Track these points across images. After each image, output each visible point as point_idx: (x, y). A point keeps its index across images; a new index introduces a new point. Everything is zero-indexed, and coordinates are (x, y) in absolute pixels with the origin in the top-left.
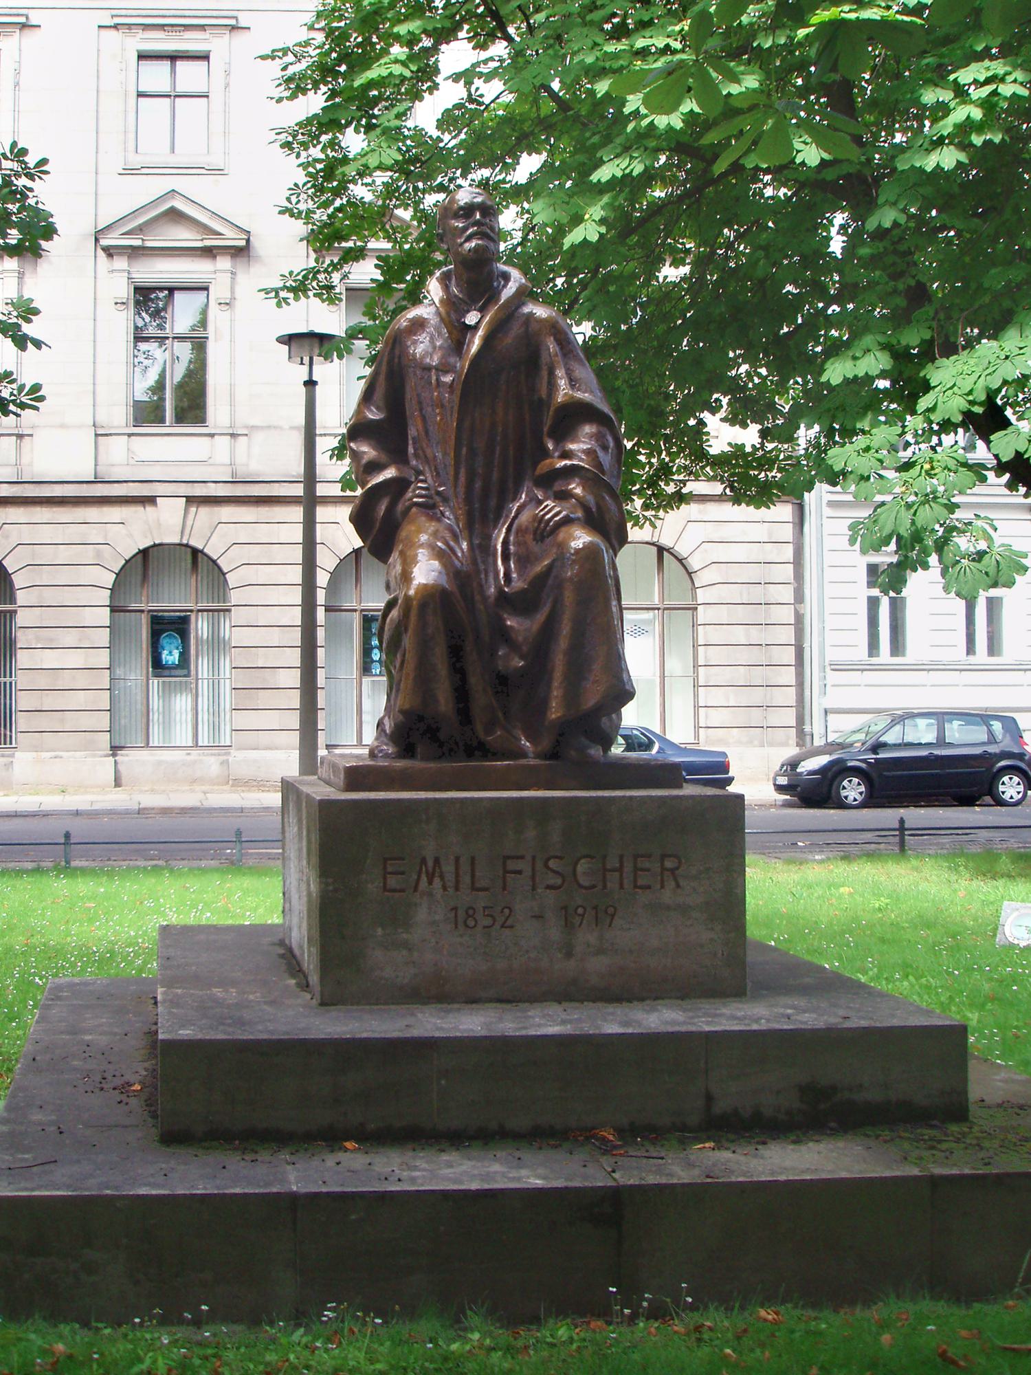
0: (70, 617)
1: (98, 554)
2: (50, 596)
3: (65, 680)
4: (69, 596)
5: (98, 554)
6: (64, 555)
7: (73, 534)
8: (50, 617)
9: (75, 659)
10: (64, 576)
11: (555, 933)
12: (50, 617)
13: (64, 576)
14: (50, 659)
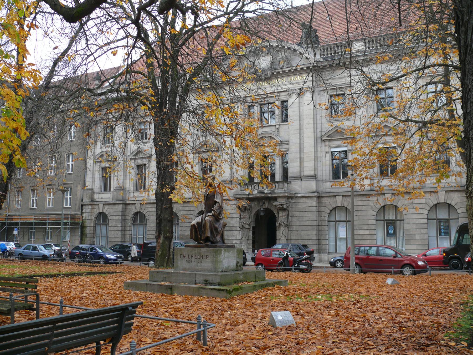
0: (366, 222)
1: (372, 207)
2: (361, 218)
3: (365, 237)
4: (365, 218)
5: (372, 207)
6: (364, 208)
7: (366, 203)
8: (361, 222)
9: (367, 232)
10: (364, 213)
11: (196, 263)
12: (361, 222)
13: (364, 213)
14: (361, 232)
